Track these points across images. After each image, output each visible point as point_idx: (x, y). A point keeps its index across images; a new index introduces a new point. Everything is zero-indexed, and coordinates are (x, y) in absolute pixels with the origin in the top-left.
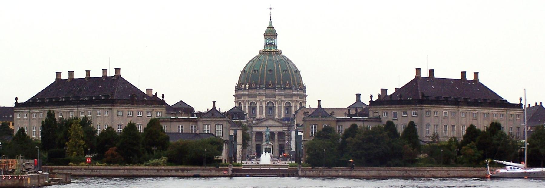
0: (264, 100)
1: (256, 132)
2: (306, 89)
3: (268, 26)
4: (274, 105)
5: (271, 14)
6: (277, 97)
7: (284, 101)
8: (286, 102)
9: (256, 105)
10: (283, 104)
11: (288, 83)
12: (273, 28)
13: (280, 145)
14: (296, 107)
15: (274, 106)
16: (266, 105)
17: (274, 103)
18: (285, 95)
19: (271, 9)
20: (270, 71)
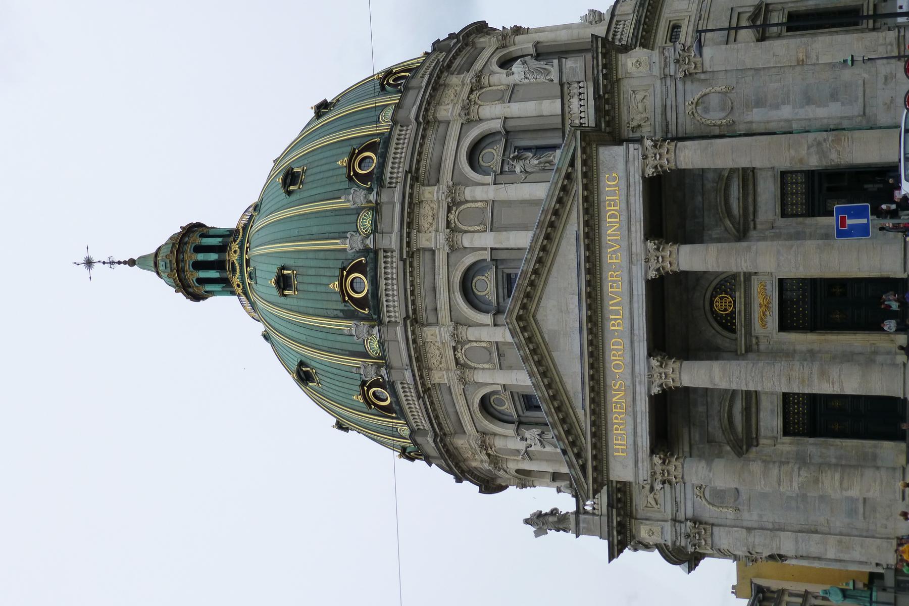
0: (447, 337)
1: (653, 452)
2: (443, 36)
3: (155, 274)
4: (486, 255)
5: (114, 263)
6: (425, 240)
7: (459, 182)
8: (467, 169)
9: (499, 388)
10: (479, 193)
11: (352, 156)
12: (159, 248)
13: (784, 215)
14: (512, 93)
15: (495, 261)
16: (487, 319)
17: (469, 260)
18: (416, 179)
19: (89, 263)
20: (283, 282)
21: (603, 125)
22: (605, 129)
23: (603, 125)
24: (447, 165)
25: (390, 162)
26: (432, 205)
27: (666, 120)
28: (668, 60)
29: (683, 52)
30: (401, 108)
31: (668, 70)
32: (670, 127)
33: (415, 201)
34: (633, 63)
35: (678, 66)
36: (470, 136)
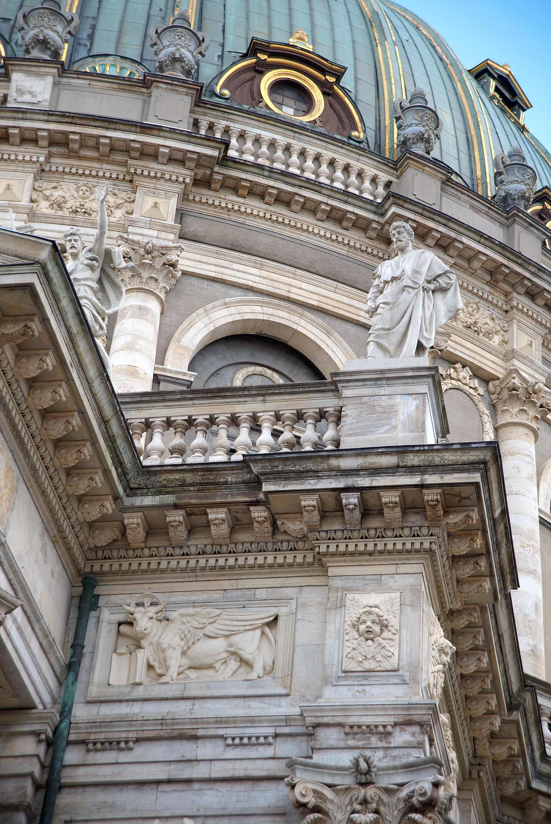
21: (148, 501)
22: (134, 509)
23: (148, 501)
24: (241, 267)
25: (278, 137)
26: (119, 214)
27: (138, 740)
28: (374, 741)
29: (401, 805)
30: (442, 189)
31: (332, 742)
32: (110, 756)
33: (137, 165)
34: (376, 607)
35: (348, 781)
36: (329, 341)
